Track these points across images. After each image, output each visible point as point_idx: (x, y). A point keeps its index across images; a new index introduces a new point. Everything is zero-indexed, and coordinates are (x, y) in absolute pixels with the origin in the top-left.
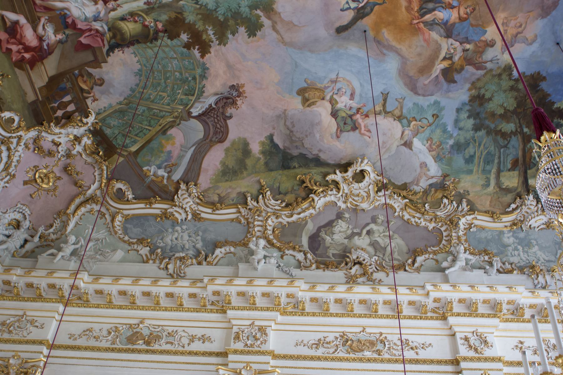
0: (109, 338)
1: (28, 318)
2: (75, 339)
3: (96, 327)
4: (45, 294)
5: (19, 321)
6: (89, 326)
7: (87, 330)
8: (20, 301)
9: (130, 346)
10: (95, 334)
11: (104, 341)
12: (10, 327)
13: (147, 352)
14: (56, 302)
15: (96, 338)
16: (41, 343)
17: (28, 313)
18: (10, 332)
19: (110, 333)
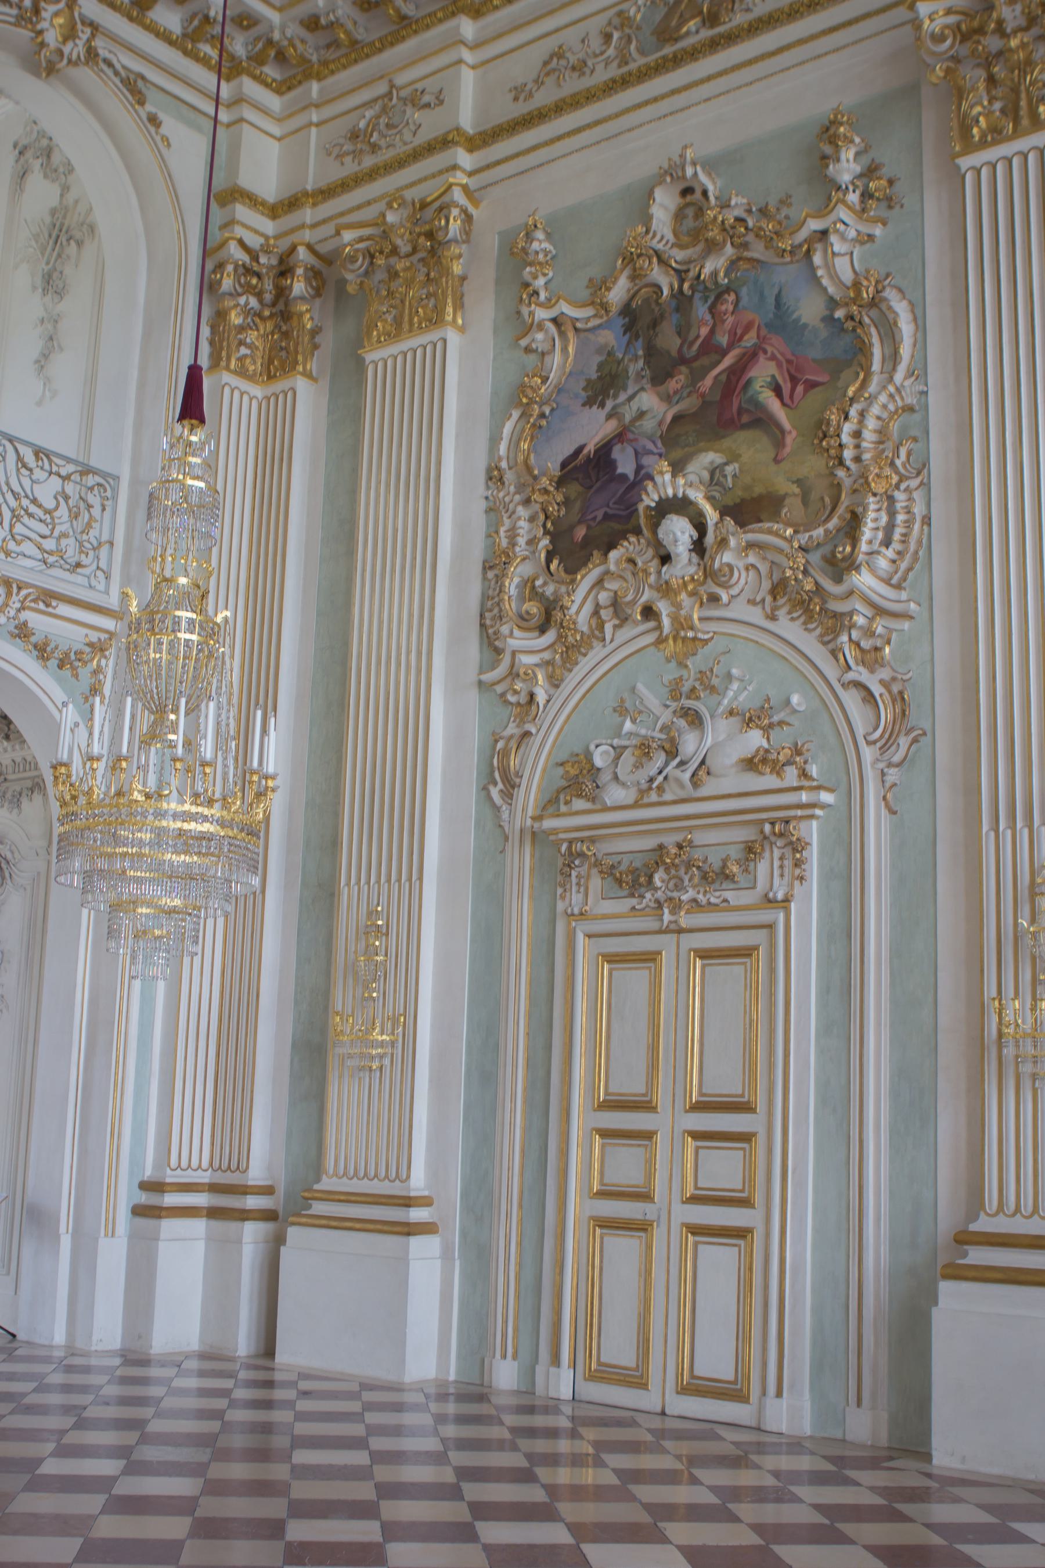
0: (611, 52)
1: (403, 93)
2: (531, 95)
3: (571, 37)
4: (412, 7)
5: (384, 110)
6: (550, 44)
7: (551, 57)
8: (367, 56)
9: (668, 50)
10: (573, 59)
11: (600, 68)
12: (371, 135)
13: (714, 45)
14: (446, 18)
15: (580, 68)
16: (444, 143)
17: (400, 80)
18: (374, 148)
19: (608, 37)
